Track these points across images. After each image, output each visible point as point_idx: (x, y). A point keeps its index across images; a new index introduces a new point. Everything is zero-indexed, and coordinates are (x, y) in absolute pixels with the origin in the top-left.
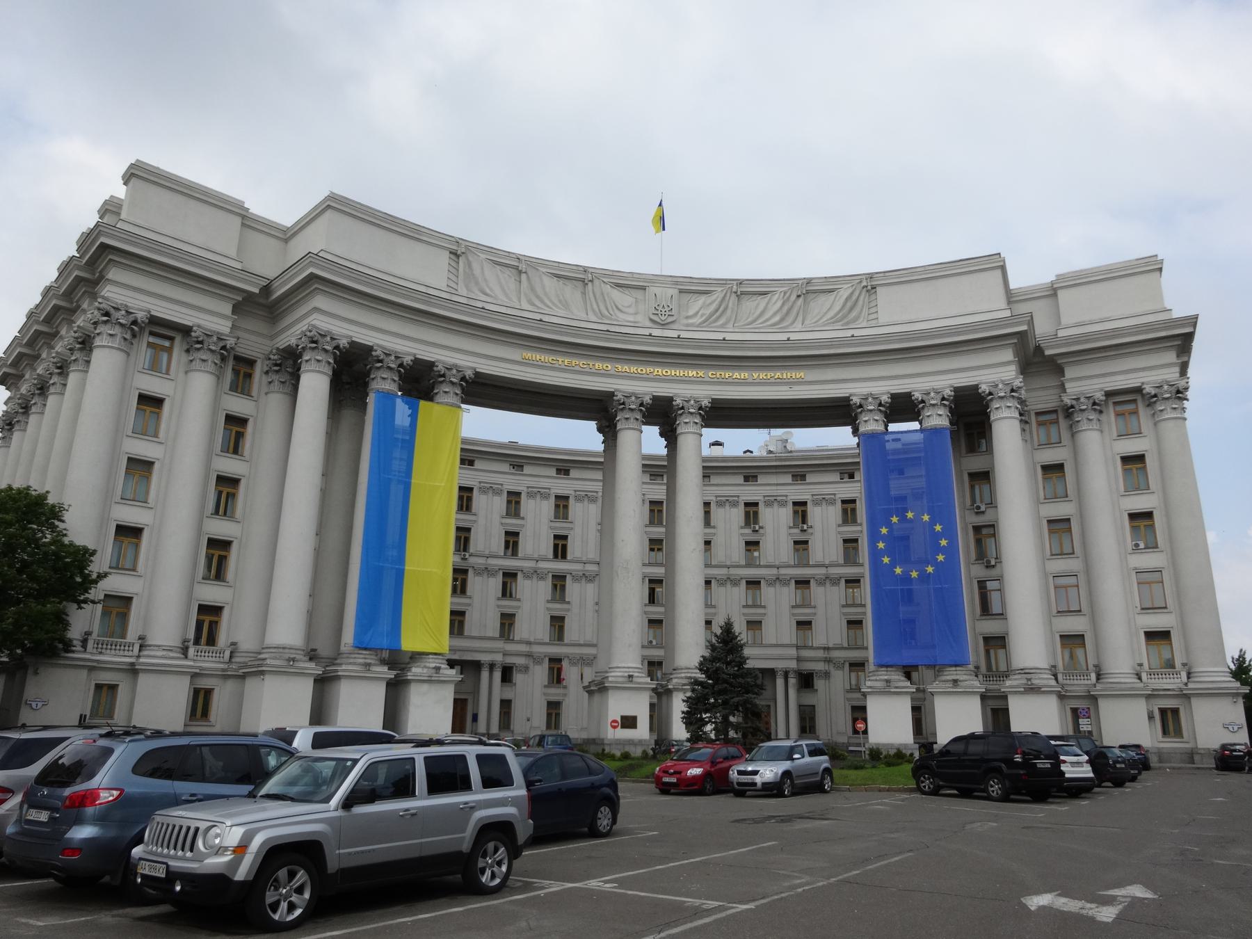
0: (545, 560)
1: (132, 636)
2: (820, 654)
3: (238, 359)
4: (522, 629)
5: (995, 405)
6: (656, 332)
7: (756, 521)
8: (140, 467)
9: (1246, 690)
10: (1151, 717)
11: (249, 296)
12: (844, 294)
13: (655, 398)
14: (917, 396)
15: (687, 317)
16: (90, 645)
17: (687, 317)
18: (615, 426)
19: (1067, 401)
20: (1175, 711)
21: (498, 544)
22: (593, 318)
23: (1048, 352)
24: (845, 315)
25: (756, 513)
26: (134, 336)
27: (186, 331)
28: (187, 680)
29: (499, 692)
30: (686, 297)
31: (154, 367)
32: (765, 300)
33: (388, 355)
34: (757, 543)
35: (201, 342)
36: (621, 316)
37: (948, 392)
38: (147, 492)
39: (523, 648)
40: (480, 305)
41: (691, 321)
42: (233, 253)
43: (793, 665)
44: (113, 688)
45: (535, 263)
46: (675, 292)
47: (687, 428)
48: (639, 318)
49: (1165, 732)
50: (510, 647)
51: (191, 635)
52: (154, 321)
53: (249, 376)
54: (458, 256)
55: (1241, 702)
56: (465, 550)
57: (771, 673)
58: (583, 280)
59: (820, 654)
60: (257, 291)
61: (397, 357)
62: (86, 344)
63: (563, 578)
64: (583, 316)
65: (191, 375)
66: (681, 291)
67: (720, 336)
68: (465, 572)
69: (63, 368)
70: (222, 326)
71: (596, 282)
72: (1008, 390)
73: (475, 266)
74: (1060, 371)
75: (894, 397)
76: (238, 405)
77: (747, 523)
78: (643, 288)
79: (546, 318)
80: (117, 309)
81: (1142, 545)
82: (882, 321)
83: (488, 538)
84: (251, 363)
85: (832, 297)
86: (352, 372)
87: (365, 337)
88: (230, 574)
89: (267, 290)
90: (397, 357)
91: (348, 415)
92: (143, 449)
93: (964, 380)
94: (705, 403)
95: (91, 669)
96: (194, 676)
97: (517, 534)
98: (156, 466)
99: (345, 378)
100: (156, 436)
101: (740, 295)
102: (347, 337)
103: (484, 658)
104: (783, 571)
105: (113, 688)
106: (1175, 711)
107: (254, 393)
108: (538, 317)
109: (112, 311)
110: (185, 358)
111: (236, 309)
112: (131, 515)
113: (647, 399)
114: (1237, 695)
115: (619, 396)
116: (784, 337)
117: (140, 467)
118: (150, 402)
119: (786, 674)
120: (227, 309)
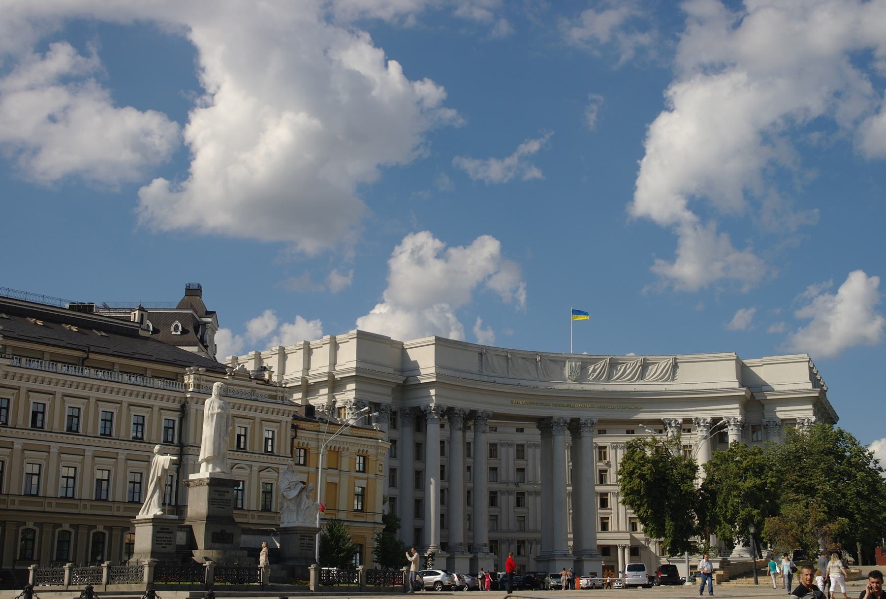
7: (605, 459)
11: (399, 384)
18: (551, 433)
19: (765, 421)
23: (757, 398)
25: (605, 453)
34: (606, 471)
37: (709, 420)
43: (628, 543)
45: (513, 353)
47: (585, 433)
57: (616, 547)
63: (496, 493)
73: (490, 359)
74: (763, 406)
76: (395, 434)
89: (405, 382)
93: (717, 414)
111: (393, 390)
113: (568, 421)
115: (555, 420)
119: (624, 548)
120: (389, 391)
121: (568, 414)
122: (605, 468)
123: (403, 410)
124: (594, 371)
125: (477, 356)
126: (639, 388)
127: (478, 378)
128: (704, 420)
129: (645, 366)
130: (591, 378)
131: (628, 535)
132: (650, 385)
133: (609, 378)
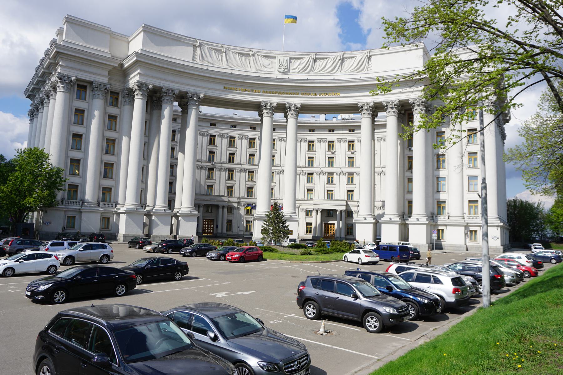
0: (246, 165)
1: (78, 198)
2: (356, 203)
3: (111, 92)
4: (236, 193)
5: (415, 108)
6: (280, 76)
8: (78, 137)
9: (502, 224)
10: (466, 234)
11: (115, 68)
12: (358, 58)
13: (278, 104)
14: (384, 104)
15: (293, 69)
16: (64, 202)
17: (293, 69)
20: (476, 231)
21: (225, 158)
22: (254, 70)
24: (358, 69)
26: (72, 86)
27: (91, 83)
28: (100, 215)
29: (226, 217)
30: (293, 61)
31: (79, 97)
32: (325, 61)
33: (169, 90)
35: (97, 87)
36: (266, 69)
38: (81, 146)
39: (236, 200)
40: (205, 68)
41: (294, 71)
42: (107, 51)
44: (74, 217)
46: (287, 58)
48: (272, 70)
49: (471, 239)
50: (231, 199)
51: (101, 199)
52: (78, 80)
53: (117, 99)
54: (197, 47)
55: (499, 228)
56: (213, 160)
57: (335, 211)
58: (249, 54)
59: (356, 203)
60: (117, 65)
61: (172, 91)
62: (55, 88)
64: (249, 69)
65: (94, 100)
66: (290, 58)
67: (305, 78)
68: (213, 169)
69: (48, 97)
70: (105, 80)
71: (256, 55)
72: (421, 101)
75: (375, 103)
77: (329, 150)
78: (274, 57)
79: (234, 72)
80: (64, 76)
81: (471, 166)
82: (372, 71)
83: (221, 155)
84: (118, 94)
85: (353, 60)
86: (154, 99)
87: (158, 83)
88: (114, 177)
90: (172, 91)
91: (155, 112)
92: (79, 130)
93: (403, 97)
94: (299, 106)
95: (65, 211)
96: (102, 213)
97: (234, 154)
98: (84, 136)
99: (154, 98)
100: (82, 124)
101: (315, 60)
102: (153, 84)
103: (220, 204)
104: (343, 170)
105: (74, 217)
106: (476, 231)
107: (119, 106)
108: (229, 71)
109: (62, 77)
110: (91, 93)
111: (110, 73)
112: (76, 155)
113: (275, 104)
114: (498, 226)
116: (331, 78)
117: (78, 137)
118: (80, 112)
120: (106, 73)
121: (275, 100)
122: (332, 156)
123: (123, 91)
124: (300, 64)
125: (191, 49)
126: (336, 78)
127: (191, 65)
128: (392, 102)
129: (343, 60)
130: (297, 70)
131: (345, 203)
132: (347, 74)
133: (312, 69)
